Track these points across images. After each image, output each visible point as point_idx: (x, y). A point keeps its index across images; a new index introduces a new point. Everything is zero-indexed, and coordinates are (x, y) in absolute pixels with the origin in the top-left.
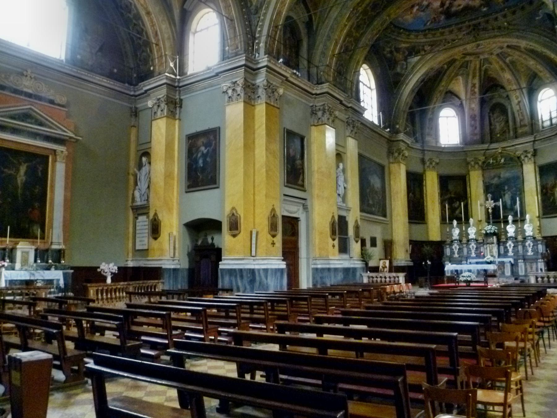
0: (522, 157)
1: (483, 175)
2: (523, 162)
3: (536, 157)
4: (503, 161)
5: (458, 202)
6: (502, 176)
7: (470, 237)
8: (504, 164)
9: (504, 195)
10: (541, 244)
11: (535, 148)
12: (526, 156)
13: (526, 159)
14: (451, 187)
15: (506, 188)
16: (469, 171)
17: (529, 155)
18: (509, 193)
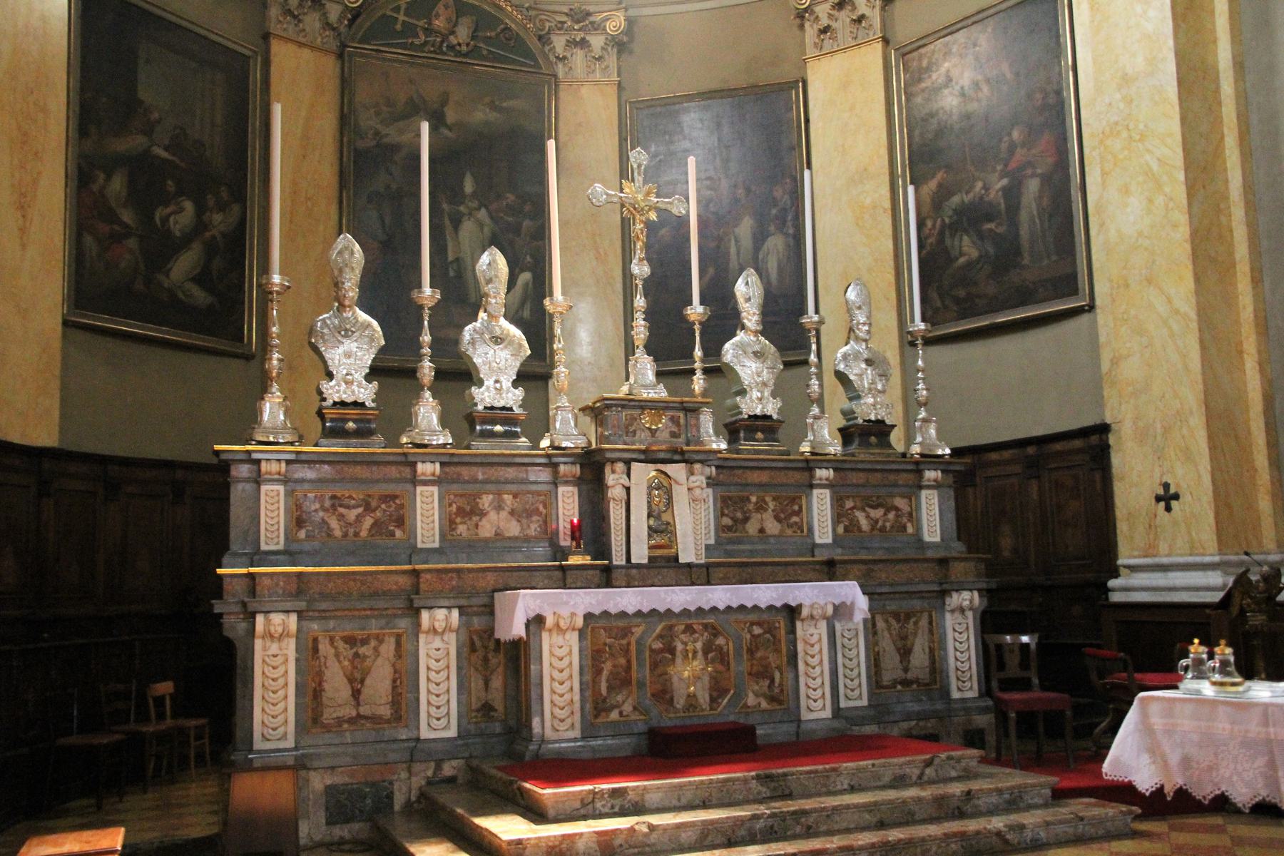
0: (559, 42)
1: (346, 84)
2: (560, 70)
3: (624, 56)
4: (463, 34)
5: (189, 206)
6: (451, 116)
7: (484, 396)
8: (474, 52)
9: (457, 223)
10: (937, 486)
11: (631, 12)
12: (583, 44)
13: (578, 57)
14: (154, 87)
15: (469, 186)
16: (266, 37)
17: (597, 41)
18: (482, 214)
